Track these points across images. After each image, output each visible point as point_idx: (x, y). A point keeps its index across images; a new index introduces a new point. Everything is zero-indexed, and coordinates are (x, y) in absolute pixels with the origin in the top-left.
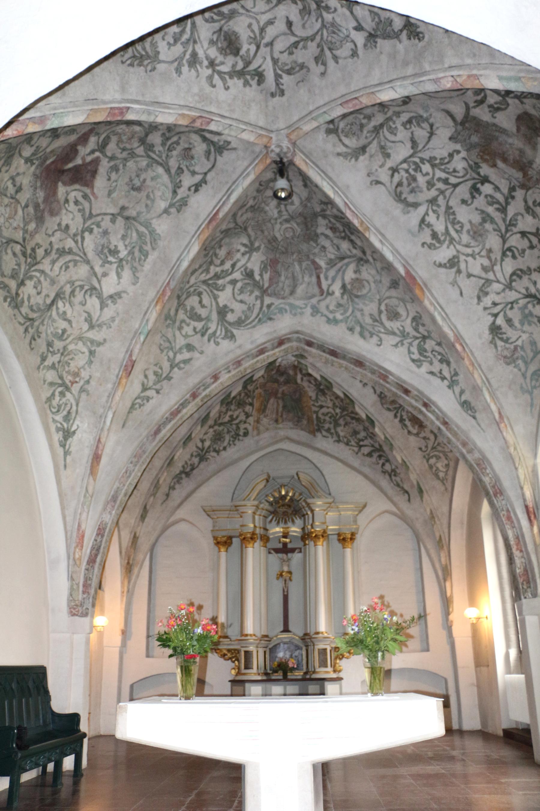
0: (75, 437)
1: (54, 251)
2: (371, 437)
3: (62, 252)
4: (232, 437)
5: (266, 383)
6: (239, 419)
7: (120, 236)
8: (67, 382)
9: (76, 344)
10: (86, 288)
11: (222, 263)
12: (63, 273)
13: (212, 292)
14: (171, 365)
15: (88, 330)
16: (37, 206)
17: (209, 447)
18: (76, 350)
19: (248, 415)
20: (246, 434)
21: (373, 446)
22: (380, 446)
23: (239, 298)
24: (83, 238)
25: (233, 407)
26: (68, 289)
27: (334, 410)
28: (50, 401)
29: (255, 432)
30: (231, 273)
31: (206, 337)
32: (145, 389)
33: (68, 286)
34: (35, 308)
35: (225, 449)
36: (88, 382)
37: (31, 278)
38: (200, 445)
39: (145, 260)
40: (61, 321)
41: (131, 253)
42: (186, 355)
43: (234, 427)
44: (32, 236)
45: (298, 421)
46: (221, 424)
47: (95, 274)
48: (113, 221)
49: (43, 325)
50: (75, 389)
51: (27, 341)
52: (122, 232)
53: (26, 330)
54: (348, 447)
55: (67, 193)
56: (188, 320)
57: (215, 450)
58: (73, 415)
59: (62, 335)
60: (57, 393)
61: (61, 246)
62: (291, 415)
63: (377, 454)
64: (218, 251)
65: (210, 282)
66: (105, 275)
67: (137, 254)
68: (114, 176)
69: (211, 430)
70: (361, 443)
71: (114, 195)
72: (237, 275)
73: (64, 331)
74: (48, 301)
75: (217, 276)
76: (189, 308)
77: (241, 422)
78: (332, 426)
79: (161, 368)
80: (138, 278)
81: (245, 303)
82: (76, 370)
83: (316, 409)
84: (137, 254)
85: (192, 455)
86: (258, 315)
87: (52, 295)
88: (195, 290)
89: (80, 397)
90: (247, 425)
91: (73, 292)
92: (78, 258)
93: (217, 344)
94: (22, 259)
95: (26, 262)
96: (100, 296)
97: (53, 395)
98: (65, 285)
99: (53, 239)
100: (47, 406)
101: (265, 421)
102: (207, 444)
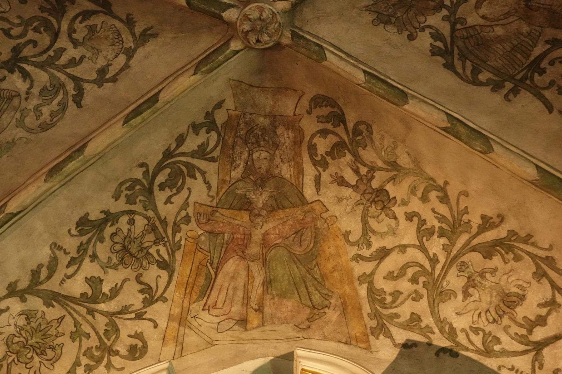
4: (88, 353)
5: (215, 210)
20: (137, 352)
25: (103, 250)
27: (423, 249)
29: (170, 349)
43: (101, 322)
46: (52, 298)
62: (289, 304)
70: (539, 334)
77: (125, 310)
83: (367, 267)
90: (144, 327)
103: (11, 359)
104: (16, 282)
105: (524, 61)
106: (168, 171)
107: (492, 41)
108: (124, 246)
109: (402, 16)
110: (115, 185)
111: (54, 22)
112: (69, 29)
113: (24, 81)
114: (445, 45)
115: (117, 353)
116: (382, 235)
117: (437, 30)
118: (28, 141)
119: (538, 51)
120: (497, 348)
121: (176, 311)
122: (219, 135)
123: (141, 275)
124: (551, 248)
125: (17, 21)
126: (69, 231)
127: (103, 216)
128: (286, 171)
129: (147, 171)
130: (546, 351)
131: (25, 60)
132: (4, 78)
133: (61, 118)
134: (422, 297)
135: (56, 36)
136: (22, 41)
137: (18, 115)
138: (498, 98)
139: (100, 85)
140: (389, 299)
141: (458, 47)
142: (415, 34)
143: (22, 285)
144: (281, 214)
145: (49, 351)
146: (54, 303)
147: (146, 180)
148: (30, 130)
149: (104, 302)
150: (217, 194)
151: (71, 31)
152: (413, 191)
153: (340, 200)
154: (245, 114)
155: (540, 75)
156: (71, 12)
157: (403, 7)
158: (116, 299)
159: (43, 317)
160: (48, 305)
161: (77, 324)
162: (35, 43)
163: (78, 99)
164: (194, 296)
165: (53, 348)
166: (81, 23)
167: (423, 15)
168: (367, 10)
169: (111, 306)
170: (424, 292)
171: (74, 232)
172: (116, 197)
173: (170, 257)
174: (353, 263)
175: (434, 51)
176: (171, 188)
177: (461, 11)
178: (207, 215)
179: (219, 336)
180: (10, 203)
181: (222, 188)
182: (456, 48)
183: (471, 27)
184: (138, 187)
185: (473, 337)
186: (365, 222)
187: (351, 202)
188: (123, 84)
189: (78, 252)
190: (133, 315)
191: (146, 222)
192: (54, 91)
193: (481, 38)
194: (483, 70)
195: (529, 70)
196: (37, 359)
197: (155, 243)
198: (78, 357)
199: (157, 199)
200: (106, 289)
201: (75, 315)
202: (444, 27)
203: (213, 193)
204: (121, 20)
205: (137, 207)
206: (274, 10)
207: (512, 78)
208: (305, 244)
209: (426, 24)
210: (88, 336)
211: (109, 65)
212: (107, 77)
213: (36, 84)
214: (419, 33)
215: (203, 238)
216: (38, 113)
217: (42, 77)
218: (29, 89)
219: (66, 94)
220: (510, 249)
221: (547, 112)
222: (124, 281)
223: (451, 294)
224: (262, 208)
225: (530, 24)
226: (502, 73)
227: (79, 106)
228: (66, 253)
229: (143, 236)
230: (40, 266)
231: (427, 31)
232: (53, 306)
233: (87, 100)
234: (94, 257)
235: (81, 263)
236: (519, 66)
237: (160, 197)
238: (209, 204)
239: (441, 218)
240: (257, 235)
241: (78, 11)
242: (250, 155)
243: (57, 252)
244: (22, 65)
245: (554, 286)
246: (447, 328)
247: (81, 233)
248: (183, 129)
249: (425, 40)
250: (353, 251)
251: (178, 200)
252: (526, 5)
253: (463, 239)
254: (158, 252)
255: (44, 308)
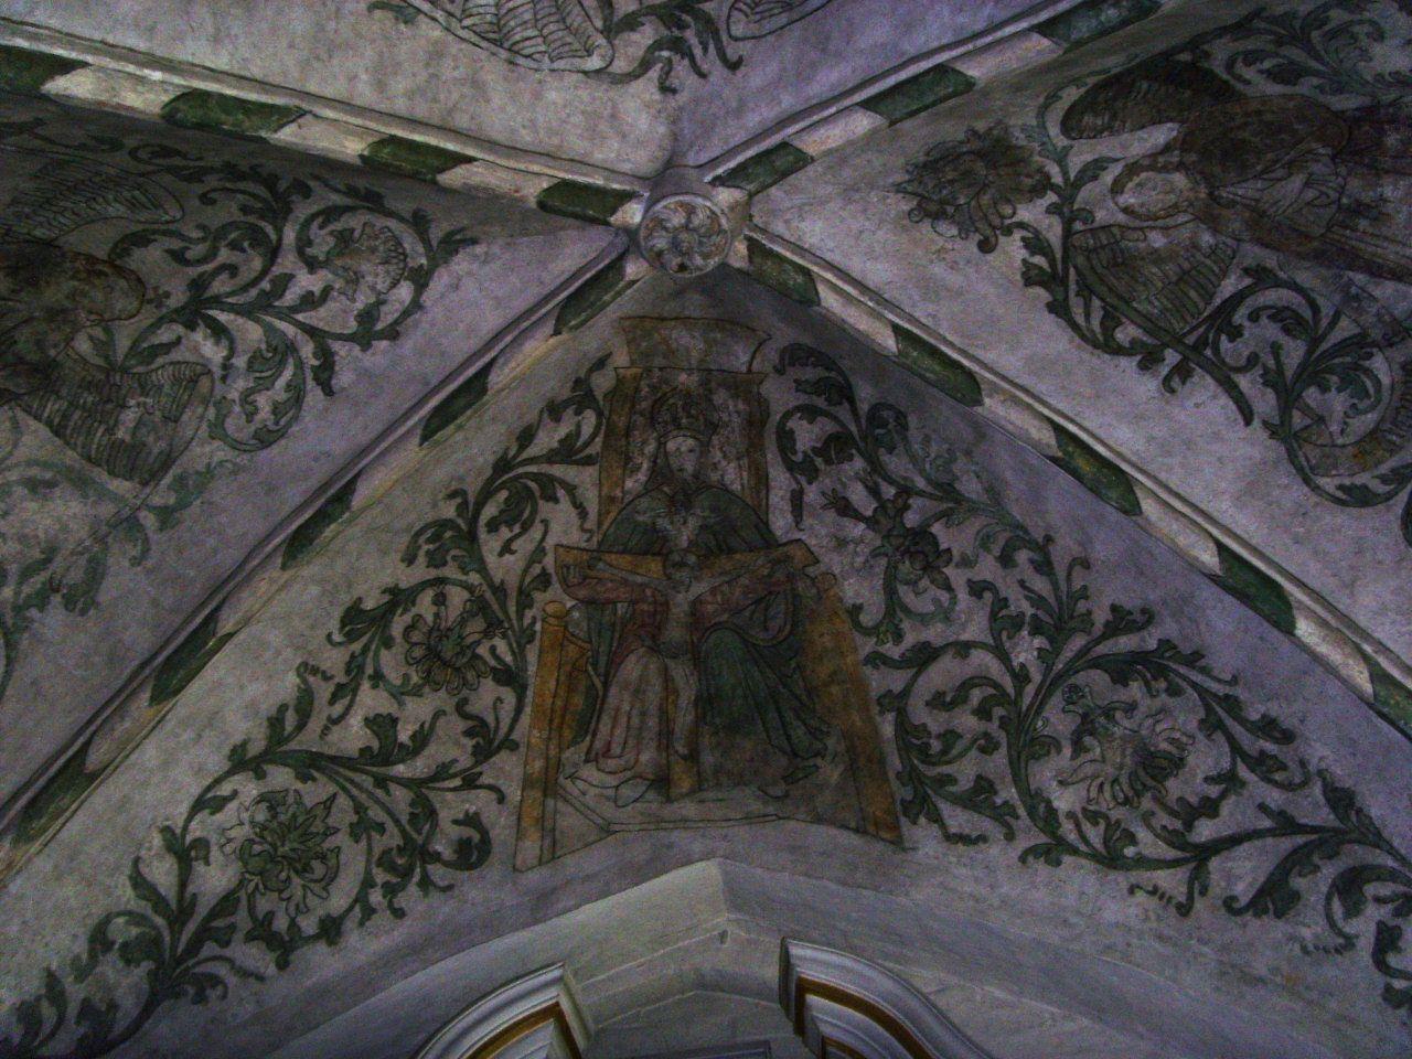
2: (1263, 765)
4: (385, 861)
17: (227, 903)
19: (486, 740)
20: (473, 852)
21: (1286, 824)
22: (1341, 799)
27: (1003, 656)
29: (531, 847)
35: (331, 930)
38: (162, 873)
43: (401, 797)
45: (790, 779)
46: (311, 765)
54: (1122, 879)
57: (262, 932)
63: (1329, 871)
69: (249, 788)
70: (1205, 831)
77: (442, 772)
78: (998, 763)
83: (896, 680)
85: (100, 939)
90: (479, 801)
101: (591, 783)
102: (215, 878)
103: (252, 884)
104: (244, 744)
105: (1201, 305)
106: (504, 494)
107: (1143, 259)
108: (429, 648)
109: (968, 203)
110: (405, 539)
111: (269, 229)
112: (298, 239)
113: (217, 343)
114: (1052, 262)
115: (437, 857)
116: (924, 620)
117: (1037, 233)
118: (237, 470)
119: (1230, 286)
120: (1130, 851)
121: (538, 765)
122: (600, 414)
123: (465, 701)
124: (1234, 681)
125: (195, 234)
126: (329, 636)
127: (387, 598)
128: (733, 476)
129: (465, 503)
130: (1214, 864)
131: (217, 301)
132: (178, 341)
133: (296, 418)
134: (996, 746)
135: (273, 253)
136: (209, 267)
137: (211, 413)
138: (1148, 386)
139: (366, 347)
140: (936, 746)
141: (1075, 267)
142: (993, 239)
143: (255, 749)
144: (724, 563)
145: (316, 864)
146: (316, 774)
147: (463, 518)
148: (236, 445)
149: (402, 761)
150: (600, 524)
151: (303, 243)
152: (985, 541)
153: (841, 543)
154: (649, 370)
155: (1232, 340)
156: (303, 210)
157: (970, 186)
158: (426, 752)
159: (299, 802)
160: (304, 777)
161: (359, 809)
162: (232, 270)
163: (326, 375)
164: (567, 733)
165: (323, 858)
166: (321, 227)
167: (1009, 201)
168: (898, 192)
169: (419, 767)
170: (1002, 737)
171: (337, 638)
172: (410, 560)
173: (515, 659)
174: (868, 670)
175: (1031, 277)
176: (510, 526)
177: (1087, 193)
178: (580, 570)
179: (622, 814)
180: (224, 613)
181: (608, 513)
182: (1072, 271)
183: (1103, 228)
184: (448, 534)
185: (1087, 827)
186: (890, 592)
187: (863, 550)
188: (408, 345)
189: (348, 672)
190: (457, 782)
191: (466, 595)
192: (277, 358)
193: (1122, 251)
194: (1124, 320)
195: (1211, 326)
196: (296, 880)
197: (487, 633)
198: (368, 872)
199: (485, 549)
200: (404, 736)
201: (355, 792)
202: (1050, 226)
203: (591, 523)
204: (402, 219)
205: (450, 571)
206: (714, 208)
207: (1177, 341)
208: (775, 624)
209: (1014, 220)
210: (381, 828)
211: (380, 303)
212: (379, 326)
213: (240, 347)
214: (1002, 239)
215: (576, 614)
216: (250, 408)
217: (251, 333)
218: (228, 358)
219: (300, 365)
220: (1161, 672)
221: (1242, 423)
222: (438, 714)
223: (1053, 744)
224: (687, 551)
225: (1215, 231)
226: (1160, 328)
227: (329, 391)
228: (327, 678)
229: (463, 622)
230: (283, 708)
231: (1018, 235)
232: (314, 779)
233: (344, 378)
234: (378, 678)
235: (355, 692)
236: (1192, 316)
237: (490, 544)
238: (584, 545)
239: (1037, 600)
240: (681, 601)
241: (315, 208)
242: (661, 444)
243: (311, 679)
244: (211, 312)
245: (1236, 750)
246: (1042, 808)
247: (351, 637)
248: (531, 417)
249: (1013, 249)
250: (867, 645)
251: (524, 546)
252: (1210, 194)
253: (1079, 641)
254: (493, 649)
255: (299, 785)
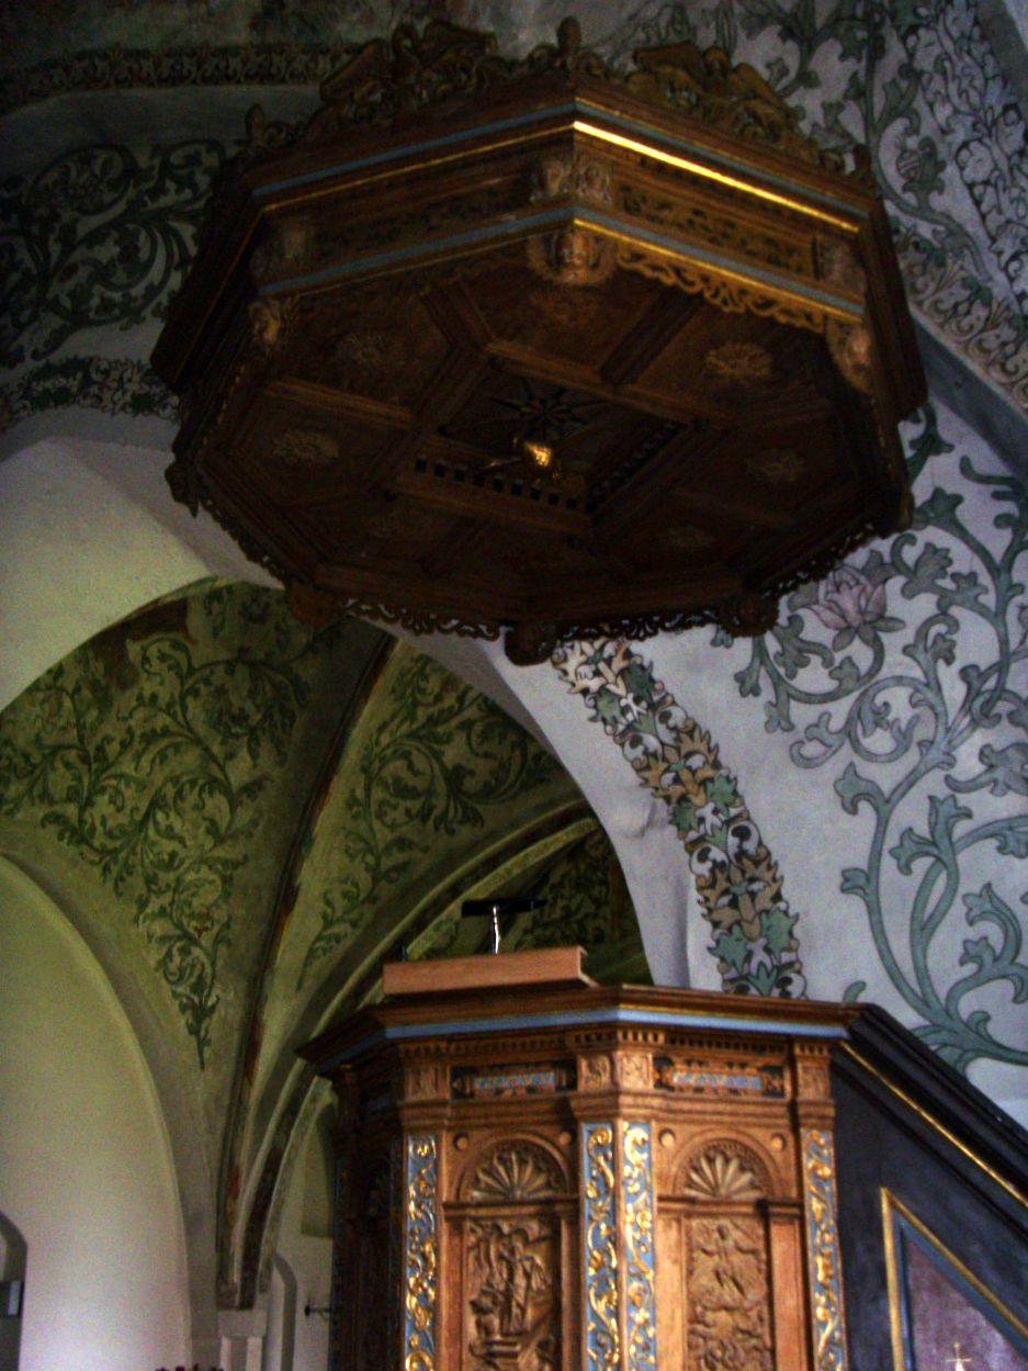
0: (215, 1016)
1: (137, 739)
3: (150, 738)
6: (583, 911)
7: (245, 693)
8: (191, 931)
9: (198, 871)
10: (201, 782)
11: (438, 698)
12: (157, 767)
13: (429, 748)
14: (374, 878)
15: (215, 846)
16: (94, 686)
18: (199, 879)
23: (481, 750)
24: (184, 708)
25: (566, 892)
26: (170, 791)
28: (165, 964)
30: (460, 710)
31: (431, 823)
32: (328, 922)
33: (170, 785)
34: (116, 833)
36: (227, 925)
37: (103, 790)
39: (291, 725)
40: (164, 841)
41: (267, 716)
42: (399, 857)
43: (575, 926)
44: (94, 730)
46: (546, 925)
47: (213, 758)
48: (230, 670)
49: (135, 854)
50: (206, 940)
51: (110, 885)
52: (247, 685)
53: (106, 869)
55: (144, 649)
56: (393, 801)
58: (208, 981)
59: (171, 862)
60: (175, 951)
61: (148, 727)
64: (422, 684)
65: (424, 732)
66: (230, 756)
67: (277, 716)
68: (216, 607)
71: (225, 632)
72: (470, 713)
73: (173, 855)
74: (138, 817)
75: (432, 721)
76: (390, 781)
77: (586, 915)
79: (356, 885)
80: (285, 754)
81: (495, 758)
82: (205, 910)
84: (277, 716)
86: (519, 774)
87: (144, 806)
88: (395, 752)
89: (216, 952)
90: (600, 922)
91: (179, 795)
92: (179, 739)
93: (451, 832)
94: (83, 768)
95: (90, 769)
96: (226, 790)
97: (169, 955)
98: (164, 785)
99: (132, 723)
100: (159, 974)
234: (562, 897)
